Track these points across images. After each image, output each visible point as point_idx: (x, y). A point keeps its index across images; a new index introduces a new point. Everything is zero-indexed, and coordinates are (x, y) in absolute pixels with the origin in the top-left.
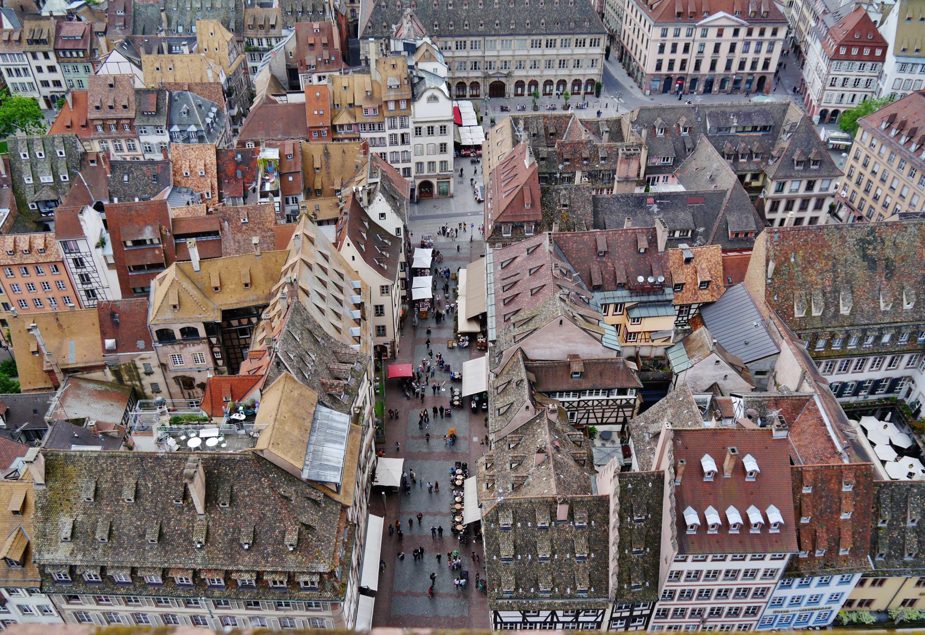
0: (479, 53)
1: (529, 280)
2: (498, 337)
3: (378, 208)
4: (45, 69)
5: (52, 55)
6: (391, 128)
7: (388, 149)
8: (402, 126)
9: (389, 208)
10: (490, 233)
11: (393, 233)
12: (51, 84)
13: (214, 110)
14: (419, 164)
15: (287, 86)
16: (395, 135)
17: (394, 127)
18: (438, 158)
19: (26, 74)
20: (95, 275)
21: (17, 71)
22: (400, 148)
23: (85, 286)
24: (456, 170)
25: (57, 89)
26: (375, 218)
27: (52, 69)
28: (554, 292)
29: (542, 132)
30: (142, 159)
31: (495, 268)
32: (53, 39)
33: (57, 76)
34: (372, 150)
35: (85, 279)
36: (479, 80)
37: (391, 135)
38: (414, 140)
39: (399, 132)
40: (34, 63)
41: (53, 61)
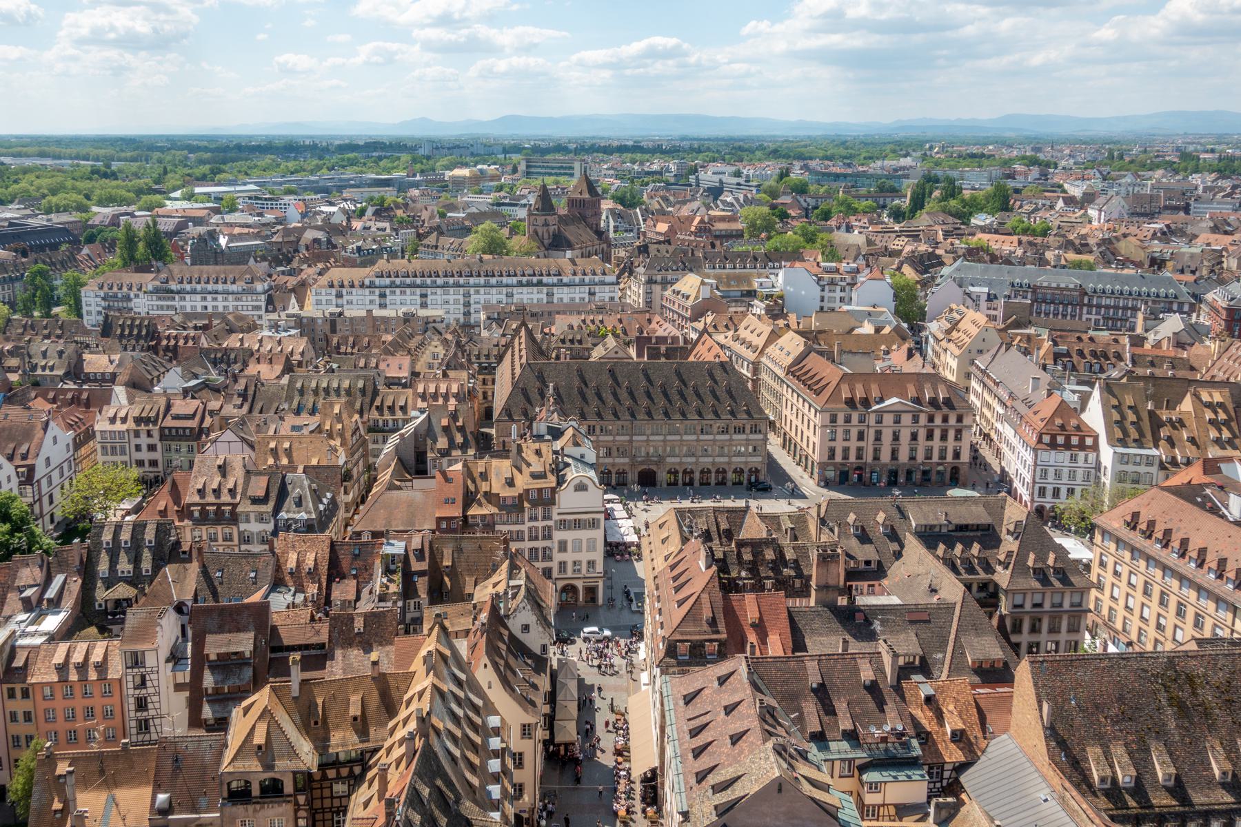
0: (627, 438)
1: (724, 722)
2: (691, 806)
3: (521, 618)
4: (144, 447)
5: (156, 434)
6: (531, 519)
7: (527, 545)
8: (545, 518)
9: (534, 618)
10: (662, 655)
11: (538, 651)
12: (147, 464)
13: (329, 495)
14: (563, 565)
15: (413, 471)
16: (537, 528)
17: (536, 519)
18: (584, 557)
19: (123, 453)
20: (155, 699)
21: (113, 448)
22: (540, 544)
23: (139, 714)
24: (605, 572)
25: (151, 469)
26: (517, 631)
27: (152, 448)
28: (765, 741)
29: (714, 528)
30: (237, 551)
31: (676, 704)
32: (161, 416)
33: (157, 455)
34: (514, 546)
35: (142, 704)
36: (626, 468)
37: (530, 529)
38: (558, 535)
39: (540, 524)
40: (135, 441)
41: (156, 440)
